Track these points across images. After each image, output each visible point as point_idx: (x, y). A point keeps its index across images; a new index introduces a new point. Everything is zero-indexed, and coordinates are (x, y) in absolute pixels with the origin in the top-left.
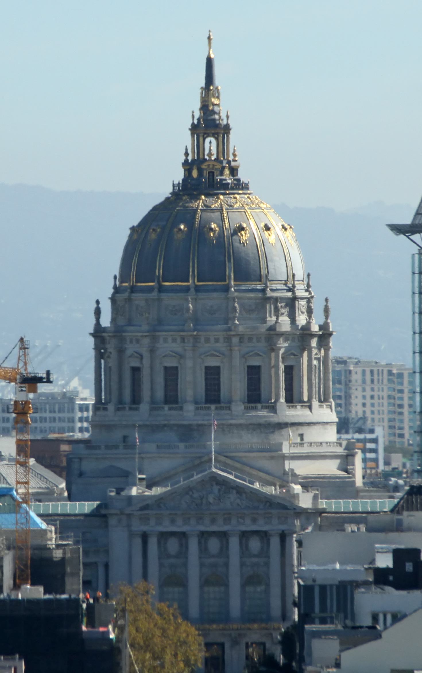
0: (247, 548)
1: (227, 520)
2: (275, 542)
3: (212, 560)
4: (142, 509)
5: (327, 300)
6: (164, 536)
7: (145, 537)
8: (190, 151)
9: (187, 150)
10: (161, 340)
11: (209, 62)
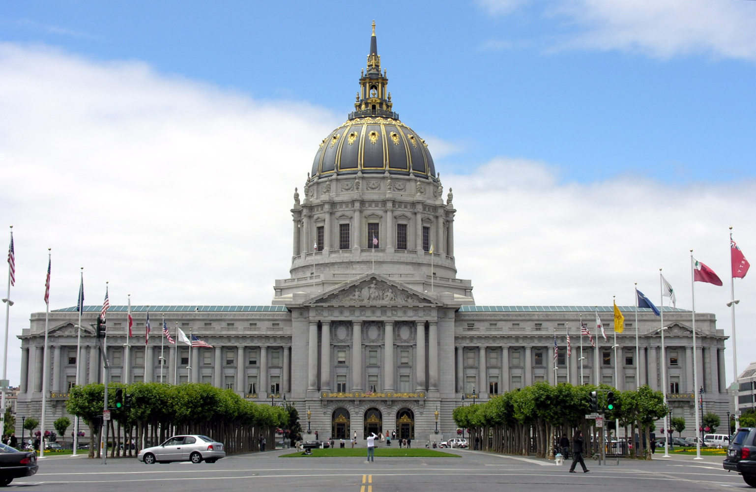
4: (317, 302)
5: (451, 190)
6: (334, 324)
7: (320, 326)
11: (374, 40)
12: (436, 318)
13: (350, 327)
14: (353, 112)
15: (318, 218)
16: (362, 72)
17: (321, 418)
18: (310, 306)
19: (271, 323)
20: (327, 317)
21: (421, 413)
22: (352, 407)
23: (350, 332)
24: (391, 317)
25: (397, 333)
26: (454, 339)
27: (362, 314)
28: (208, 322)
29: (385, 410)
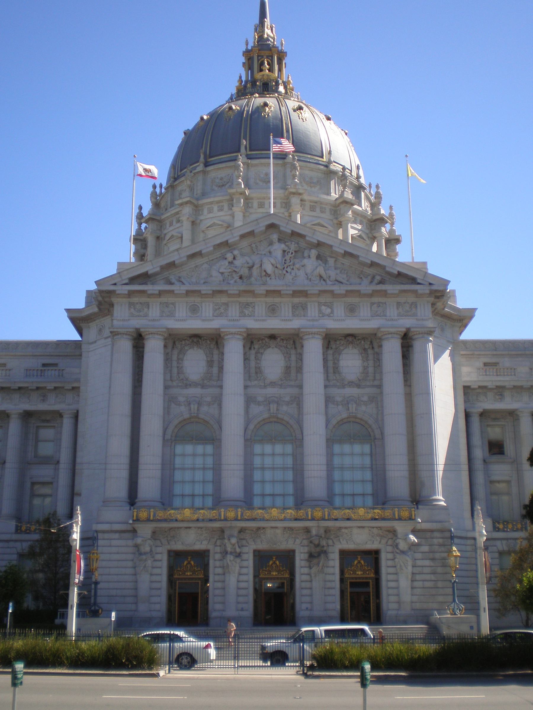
0: (336, 370)
1: (299, 310)
2: (392, 350)
3: (270, 391)
4: (133, 280)
7: (139, 340)
8: (244, 79)
9: (240, 77)
10: (205, 211)
14: (232, 95)
15: (172, 236)
16: (247, 45)
18: (114, 291)
25: (330, 364)
27: (247, 312)
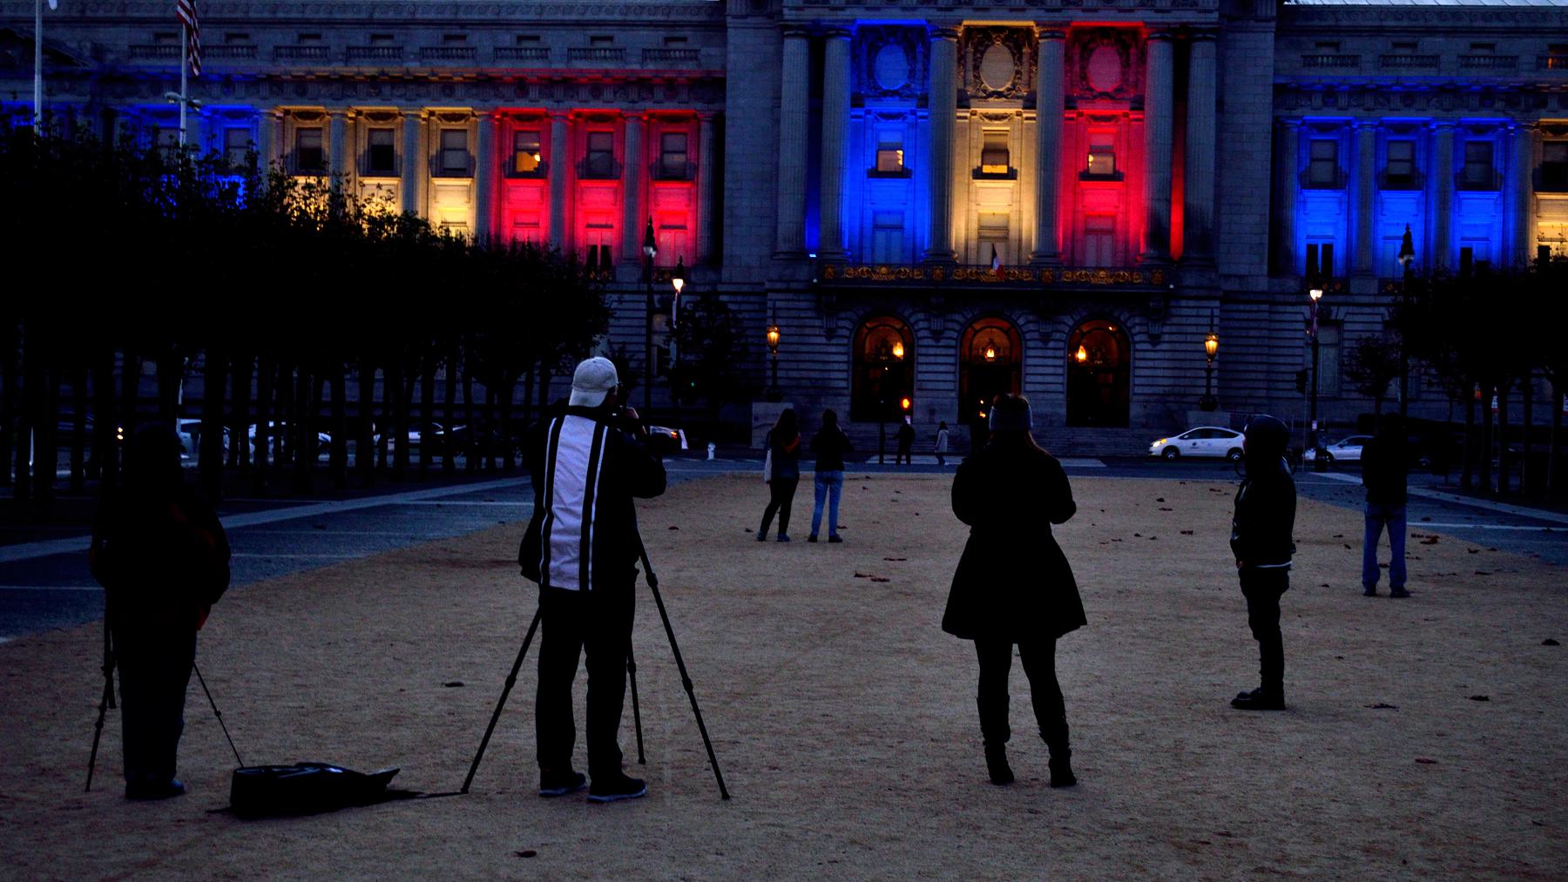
12: (1216, 15)
13: (920, 49)
17: (817, 348)
19: (663, 33)
20: (842, 9)
21: (1155, 340)
22: (921, 316)
23: (919, 66)
24: (1059, 10)
26: (1270, 90)
28: (457, 31)
29: (1031, 327)
